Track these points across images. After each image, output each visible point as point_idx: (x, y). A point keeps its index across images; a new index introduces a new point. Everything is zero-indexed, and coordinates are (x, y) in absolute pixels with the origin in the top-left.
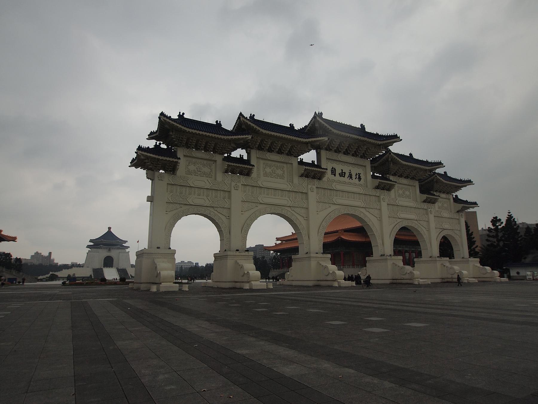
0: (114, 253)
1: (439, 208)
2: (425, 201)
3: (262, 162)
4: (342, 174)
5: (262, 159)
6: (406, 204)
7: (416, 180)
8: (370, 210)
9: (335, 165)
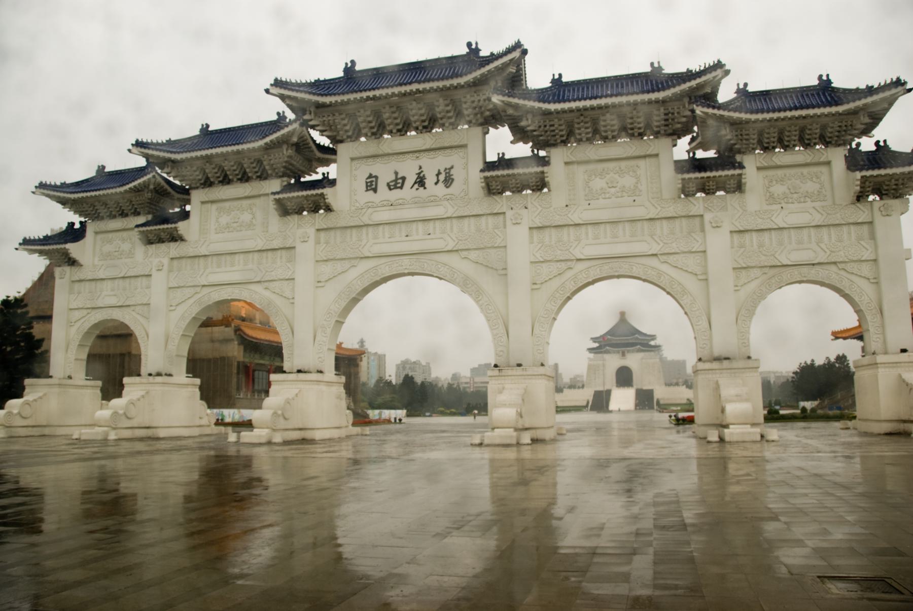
0: (634, 360)
1: (771, 199)
2: (708, 192)
3: (214, 206)
4: (397, 183)
5: (212, 202)
8: (473, 255)
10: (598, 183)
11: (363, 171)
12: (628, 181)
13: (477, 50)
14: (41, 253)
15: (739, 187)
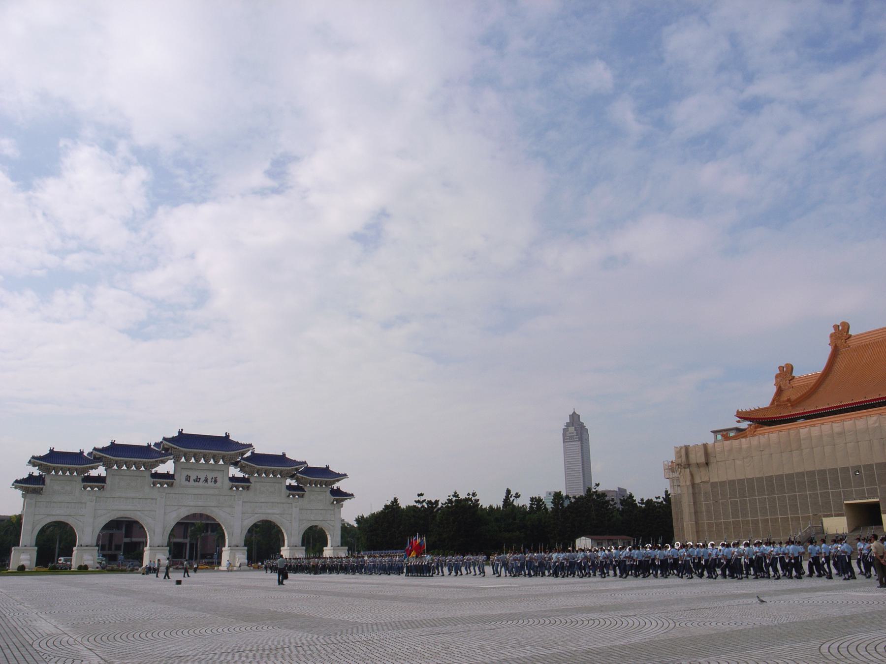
4: (197, 480)
6: (263, 500)
11: (185, 473)
14: (21, 488)
15: (302, 496)
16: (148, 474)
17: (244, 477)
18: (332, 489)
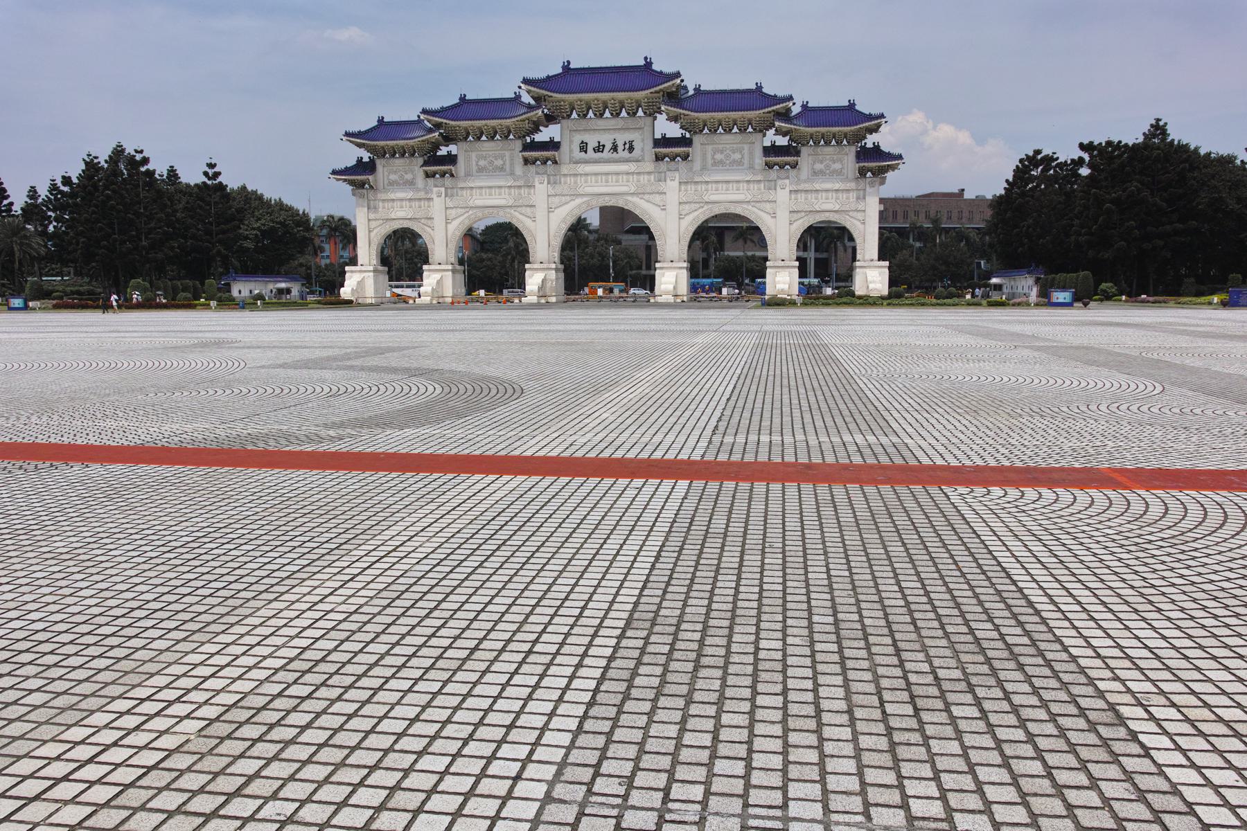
3: (474, 155)
4: (599, 148)
7: (761, 131)
8: (646, 197)
9: (586, 137)
10: (719, 157)
11: (578, 139)
12: (737, 156)
13: (651, 63)
14: (345, 180)
15: (794, 166)
16: (518, 145)
17: (683, 137)
18: (864, 148)
